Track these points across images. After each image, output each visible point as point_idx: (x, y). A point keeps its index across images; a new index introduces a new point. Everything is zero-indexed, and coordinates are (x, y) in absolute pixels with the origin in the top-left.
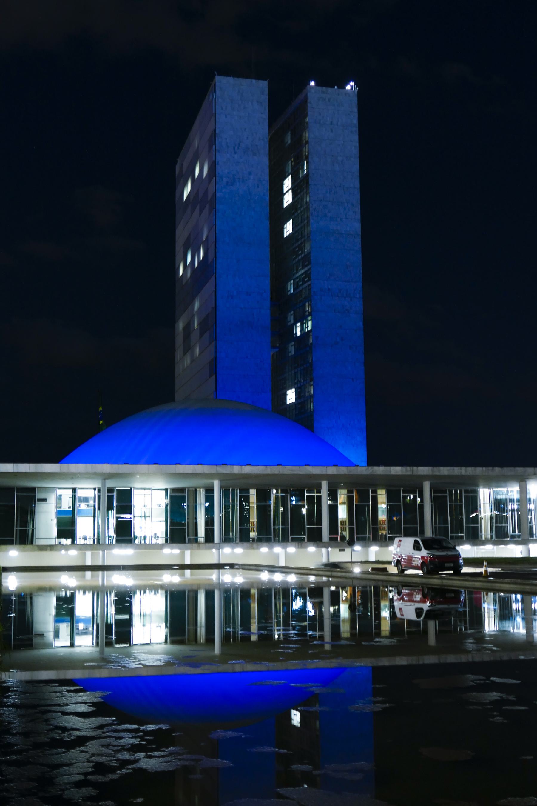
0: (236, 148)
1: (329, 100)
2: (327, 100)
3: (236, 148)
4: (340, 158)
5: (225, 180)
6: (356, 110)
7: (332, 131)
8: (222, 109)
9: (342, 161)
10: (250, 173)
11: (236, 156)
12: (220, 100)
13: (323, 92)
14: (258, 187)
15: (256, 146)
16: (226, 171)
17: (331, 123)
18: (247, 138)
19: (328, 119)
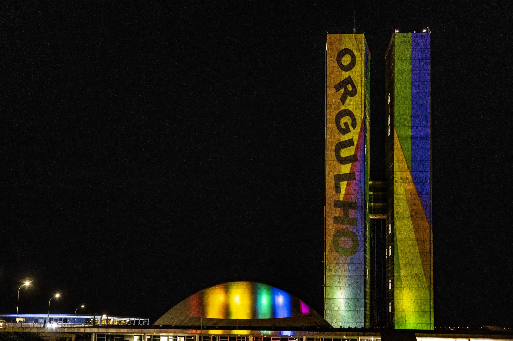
2: (407, 42)
5: (333, 106)
8: (331, 57)
9: (418, 86)
13: (404, 37)
16: (334, 101)
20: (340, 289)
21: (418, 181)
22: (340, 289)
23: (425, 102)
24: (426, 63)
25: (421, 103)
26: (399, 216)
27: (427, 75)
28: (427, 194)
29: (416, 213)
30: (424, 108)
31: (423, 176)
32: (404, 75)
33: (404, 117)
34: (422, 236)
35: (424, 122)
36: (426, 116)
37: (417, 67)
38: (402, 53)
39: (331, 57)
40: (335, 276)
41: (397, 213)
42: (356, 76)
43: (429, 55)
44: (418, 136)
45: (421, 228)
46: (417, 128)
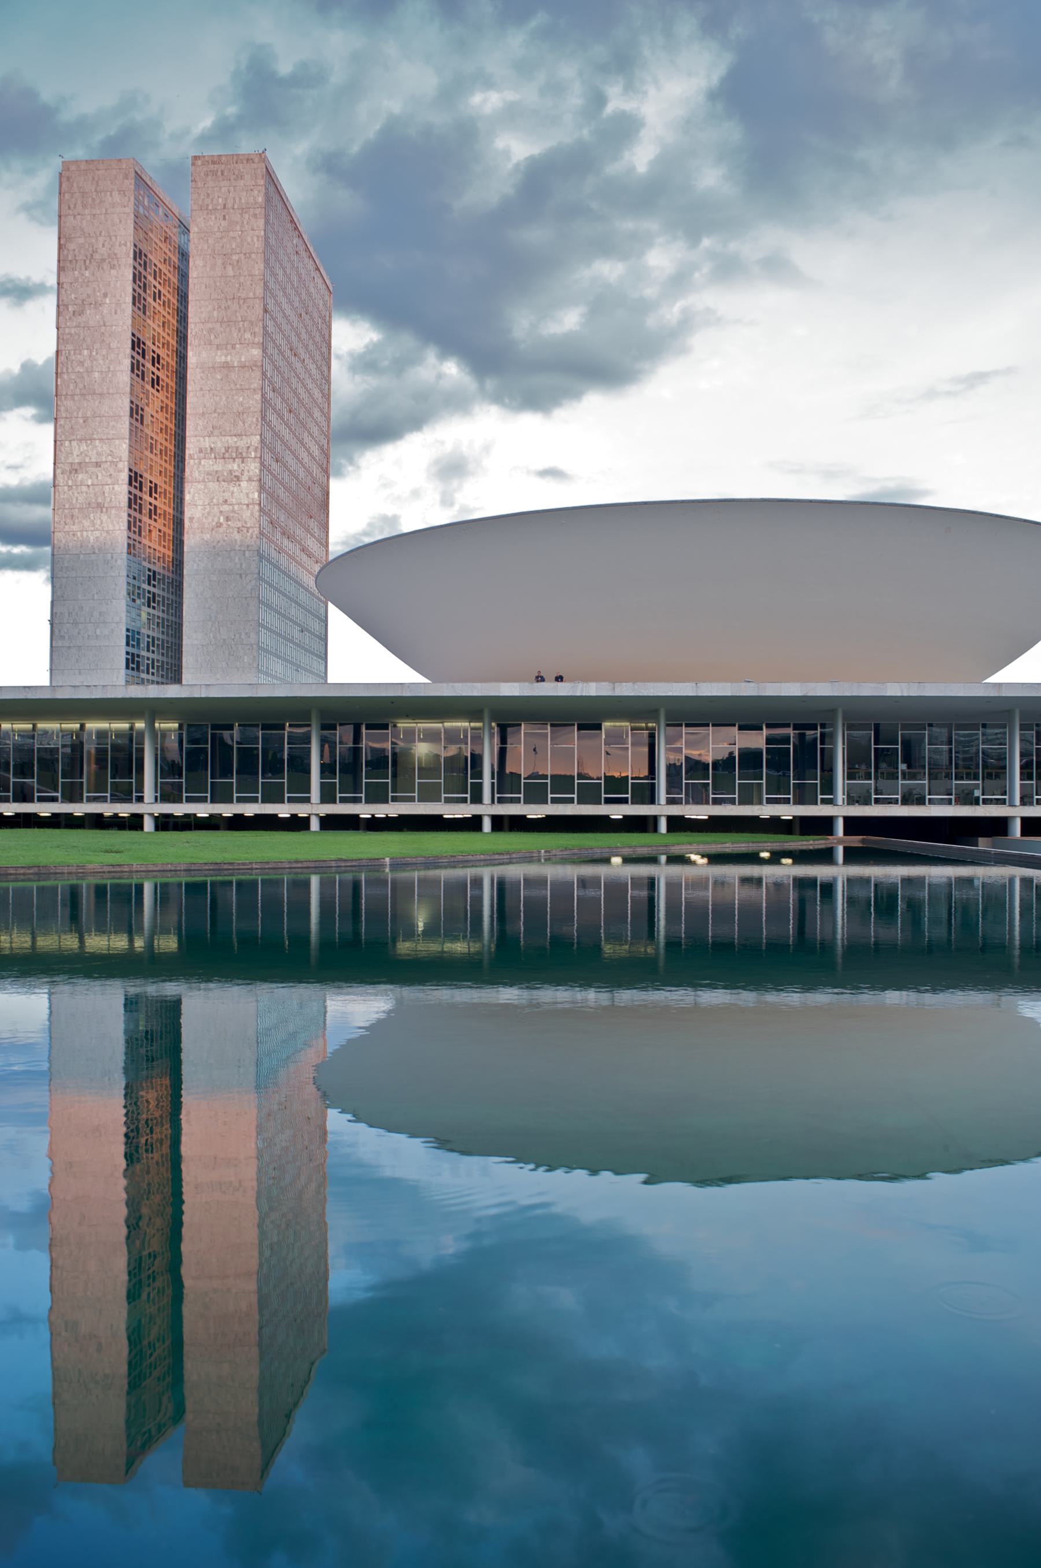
0: (88, 262)
1: (222, 172)
2: (219, 173)
3: (88, 262)
4: (235, 257)
5: (71, 309)
6: (262, 182)
7: (224, 218)
8: (69, 208)
10: (105, 295)
11: (87, 274)
12: (67, 196)
14: (116, 313)
15: (115, 254)
16: (73, 296)
17: (225, 207)
18: (103, 245)
19: (220, 200)
20: (80, 674)
21: (234, 455)
22: (80, 674)
23: (251, 295)
24: (255, 216)
25: (243, 296)
26: (196, 525)
27: (255, 239)
28: (250, 480)
29: (227, 519)
30: (248, 307)
31: (242, 443)
32: (211, 241)
33: (210, 325)
34: (238, 566)
35: (248, 336)
36: (251, 323)
37: (237, 223)
38: (208, 195)
39: (69, 208)
40: (69, 647)
41: (191, 519)
42: (117, 244)
43: (260, 199)
44: (236, 364)
45: (237, 548)
46: (233, 347)
